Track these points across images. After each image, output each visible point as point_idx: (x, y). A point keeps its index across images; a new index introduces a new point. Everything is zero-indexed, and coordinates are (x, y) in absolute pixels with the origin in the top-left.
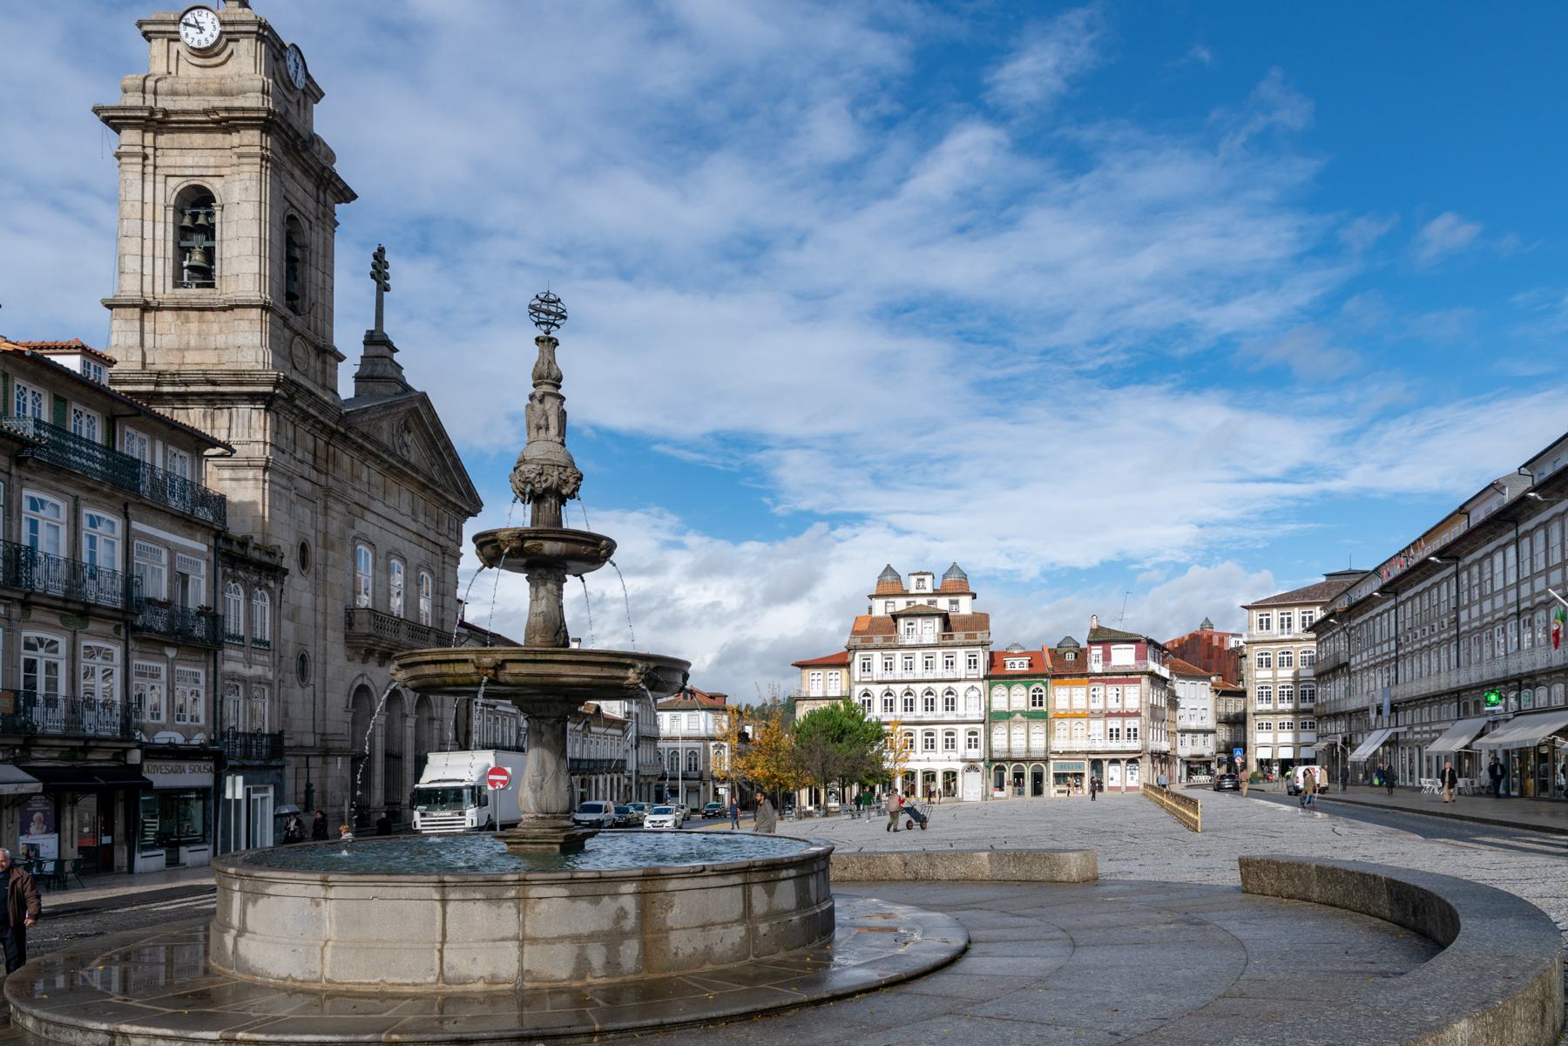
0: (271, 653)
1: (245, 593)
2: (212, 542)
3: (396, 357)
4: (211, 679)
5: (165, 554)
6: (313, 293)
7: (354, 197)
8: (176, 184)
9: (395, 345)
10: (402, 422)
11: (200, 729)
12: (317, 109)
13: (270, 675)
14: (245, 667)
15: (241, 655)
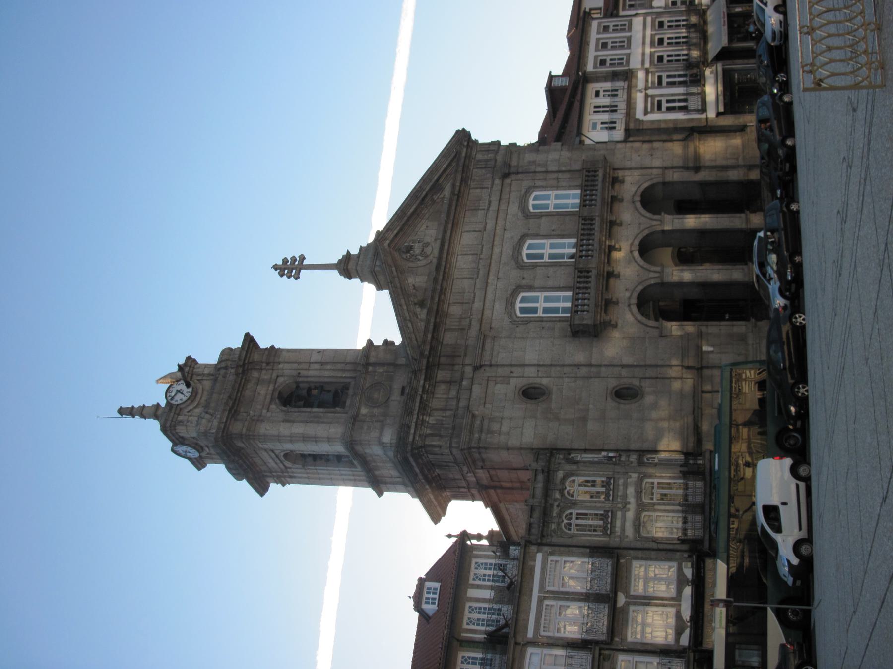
0: (616, 476)
1: (570, 508)
2: (533, 548)
3: (355, 251)
4: (640, 553)
5: (546, 602)
6: (327, 374)
7: (247, 335)
8: (288, 464)
9: (345, 253)
10: (404, 256)
11: (680, 570)
12: (201, 361)
13: (634, 476)
14: (629, 510)
15: (619, 514)
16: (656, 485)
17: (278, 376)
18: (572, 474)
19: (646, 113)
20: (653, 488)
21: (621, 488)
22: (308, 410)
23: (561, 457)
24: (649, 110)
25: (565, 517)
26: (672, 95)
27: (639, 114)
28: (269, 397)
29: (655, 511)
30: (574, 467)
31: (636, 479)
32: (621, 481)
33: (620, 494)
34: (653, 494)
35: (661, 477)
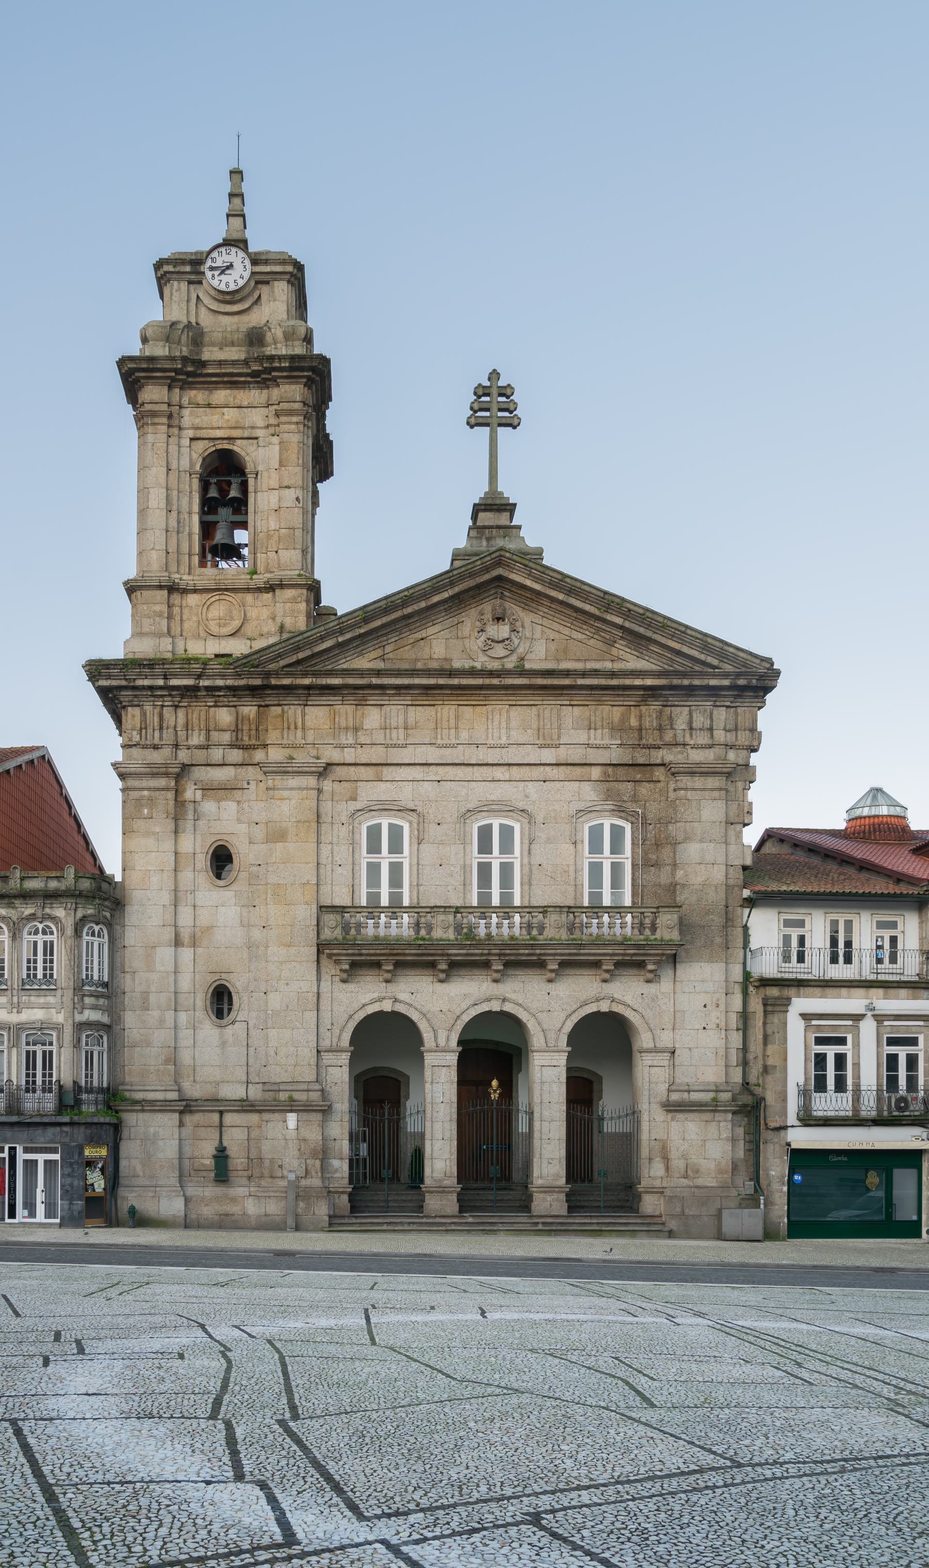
13: (60, 1018)
16: (47, 1048)
17: (256, 438)
18: (62, 931)
19: (806, 1017)
20: (44, 1044)
21: (42, 1000)
22: (196, 508)
23: (90, 912)
24: (814, 1022)
25: (46, 926)
26: (856, 1065)
27: (802, 1004)
28: (219, 434)
29: (10, 1048)
30: (69, 931)
31: (55, 1020)
32: (51, 999)
33: (32, 998)
34: (34, 1044)
35: (59, 1055)
